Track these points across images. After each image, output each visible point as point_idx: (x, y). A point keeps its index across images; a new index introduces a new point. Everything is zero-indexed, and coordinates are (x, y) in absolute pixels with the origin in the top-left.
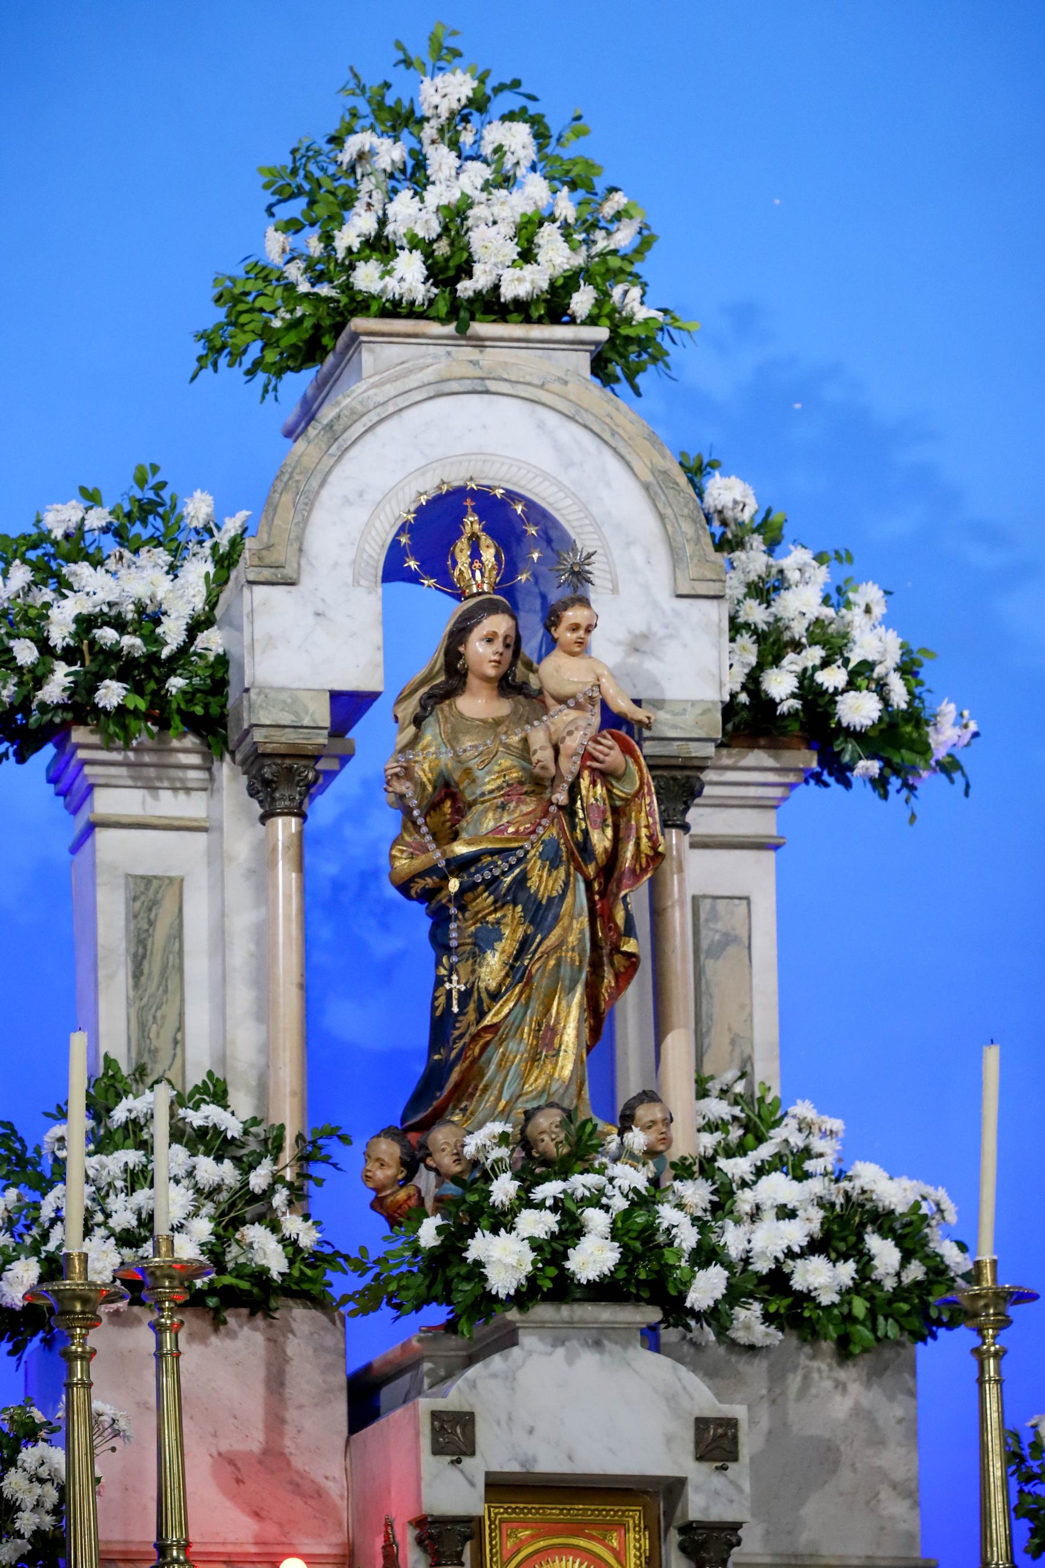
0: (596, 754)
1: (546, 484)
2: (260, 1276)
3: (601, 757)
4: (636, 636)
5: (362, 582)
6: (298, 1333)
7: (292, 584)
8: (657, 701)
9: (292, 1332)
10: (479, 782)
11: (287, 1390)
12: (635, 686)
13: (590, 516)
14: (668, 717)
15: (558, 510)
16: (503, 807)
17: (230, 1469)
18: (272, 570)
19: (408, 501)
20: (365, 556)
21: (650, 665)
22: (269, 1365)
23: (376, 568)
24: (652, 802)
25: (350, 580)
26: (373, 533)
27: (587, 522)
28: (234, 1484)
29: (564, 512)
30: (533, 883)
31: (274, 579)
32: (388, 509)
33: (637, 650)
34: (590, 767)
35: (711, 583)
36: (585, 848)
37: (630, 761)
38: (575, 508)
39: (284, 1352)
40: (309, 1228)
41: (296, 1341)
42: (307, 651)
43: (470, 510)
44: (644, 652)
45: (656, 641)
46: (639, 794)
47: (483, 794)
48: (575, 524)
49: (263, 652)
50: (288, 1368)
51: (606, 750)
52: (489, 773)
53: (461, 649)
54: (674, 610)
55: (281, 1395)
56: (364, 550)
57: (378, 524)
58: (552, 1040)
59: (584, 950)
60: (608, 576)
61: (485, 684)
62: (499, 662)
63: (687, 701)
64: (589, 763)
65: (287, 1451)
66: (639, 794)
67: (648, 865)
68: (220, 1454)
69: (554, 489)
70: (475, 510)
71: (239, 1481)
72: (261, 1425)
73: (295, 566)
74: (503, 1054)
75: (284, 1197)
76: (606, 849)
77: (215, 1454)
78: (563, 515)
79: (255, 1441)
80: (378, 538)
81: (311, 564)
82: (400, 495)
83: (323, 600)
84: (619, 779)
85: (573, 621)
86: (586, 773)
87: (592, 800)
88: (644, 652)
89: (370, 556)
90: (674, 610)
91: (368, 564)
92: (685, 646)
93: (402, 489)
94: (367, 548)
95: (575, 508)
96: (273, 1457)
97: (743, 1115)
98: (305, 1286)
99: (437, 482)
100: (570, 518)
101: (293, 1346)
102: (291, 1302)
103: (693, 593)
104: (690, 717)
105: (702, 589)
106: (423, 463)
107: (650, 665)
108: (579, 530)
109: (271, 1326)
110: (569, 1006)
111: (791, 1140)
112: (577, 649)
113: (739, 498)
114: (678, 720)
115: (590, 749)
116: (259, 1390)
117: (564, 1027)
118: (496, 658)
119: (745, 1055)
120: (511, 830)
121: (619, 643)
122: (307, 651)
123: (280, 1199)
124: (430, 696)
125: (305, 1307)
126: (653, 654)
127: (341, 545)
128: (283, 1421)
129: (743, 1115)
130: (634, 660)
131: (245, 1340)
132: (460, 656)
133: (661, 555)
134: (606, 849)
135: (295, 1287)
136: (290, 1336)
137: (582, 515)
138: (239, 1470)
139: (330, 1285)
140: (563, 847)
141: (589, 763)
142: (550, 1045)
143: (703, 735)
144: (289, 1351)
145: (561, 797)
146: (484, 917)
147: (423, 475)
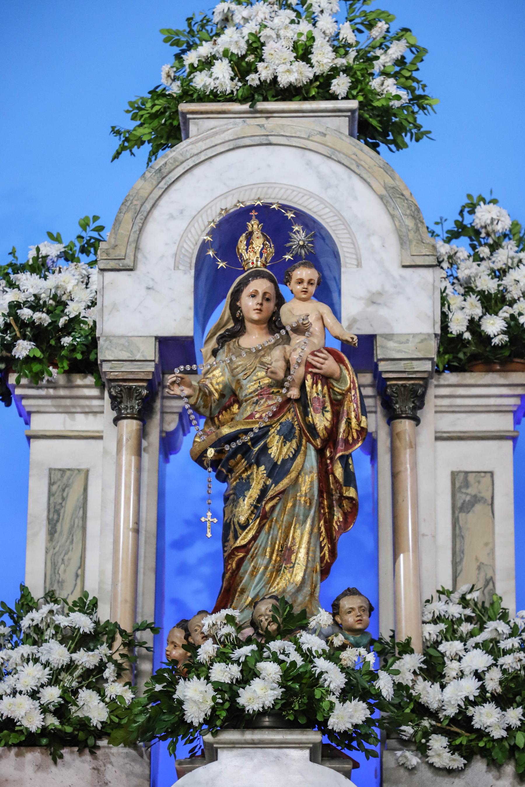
0: (314, 363)
1: (312, 200)
3: (318, 365)
5: (181, 267)
7: (131, 270)
8: (388, 335)
10: (244, 388)
12: (371, 325)
13: (342, 218)
14: (396, 345)
15: (320, 216)
16: (257, 402)
18: (116, 261)
19: (214, 215)
20: (183, 251)
23: (191, 258)
24: (356, 393)
25: (172, 267)
26: (190, 236)
27: (340, 222)
29: (324, 217)
30: (273, 451)
31: (117, 267)
32: (200, 220)
34: (311, 372)
35: (426, 257)
36: (312, 428)
37: (343, 368)
38: (331, 214)
42: (140, 312)
43: (254, 217)
45: (393, 299)
46: (349, 390)
47: (246, 395)
48: (331, 224)
49: (110, 314)
51: (321, 360)
52: (250, 381)
53: (238, 304)
54: (401, 276)
56: (183, 247)
57: (193, 230)
58: (290, 557)
59: (313, 495)
60: (354, 256)
61: (255, 326)
62: (260, 310)
63: (409, 334)
64: (310, 370)
66: (349, 390)
67: (358, 437)
69: (317, 203)
70: (257, 217)
73: (132, 258)
74: (254, 567)
76: (326, 428)
78: (324, 219)
80: (192, 240)
81: (145, 257)
82: (209, 211)
83: (153, 280)
84: (337, 380)
85: (299, 277)
86: (309, 377)
87: (315, 395)
88: (379, 304)
89: (187, 251)
90: (401, 276)
91: (185, 255)
92: (409, 299)
93: (211, 207)
94: (185, 246)
95: (331, 214)
97: (473, 615)
99: (235, 202)
100: (328, 221)
103: (413, 264)
104: (411, 345)
105: (419, 261)
106: (226, 191)
108: (334, 228)
110: (302, 534)
111: (499, 629)
112: (304, 296)
113: (495, 217)
114: (402, 347)
115: (310, 360)
117: (299, 548)
118: (258, 307)
119: (488, 577)
120: (257, 416)
122: (140, 312)
124: (222, 337)
127: (167, 244)
129: (473, 615)
132: (239, 308)
133: (393, 241)
134: (326, 428)
137: (336, 218)
140: (297, 428)
141: (310, 370)
142: (289, 560)
143: (420, 356)
145: (294, 393)
146: (240, 475)
147: (225, 198)
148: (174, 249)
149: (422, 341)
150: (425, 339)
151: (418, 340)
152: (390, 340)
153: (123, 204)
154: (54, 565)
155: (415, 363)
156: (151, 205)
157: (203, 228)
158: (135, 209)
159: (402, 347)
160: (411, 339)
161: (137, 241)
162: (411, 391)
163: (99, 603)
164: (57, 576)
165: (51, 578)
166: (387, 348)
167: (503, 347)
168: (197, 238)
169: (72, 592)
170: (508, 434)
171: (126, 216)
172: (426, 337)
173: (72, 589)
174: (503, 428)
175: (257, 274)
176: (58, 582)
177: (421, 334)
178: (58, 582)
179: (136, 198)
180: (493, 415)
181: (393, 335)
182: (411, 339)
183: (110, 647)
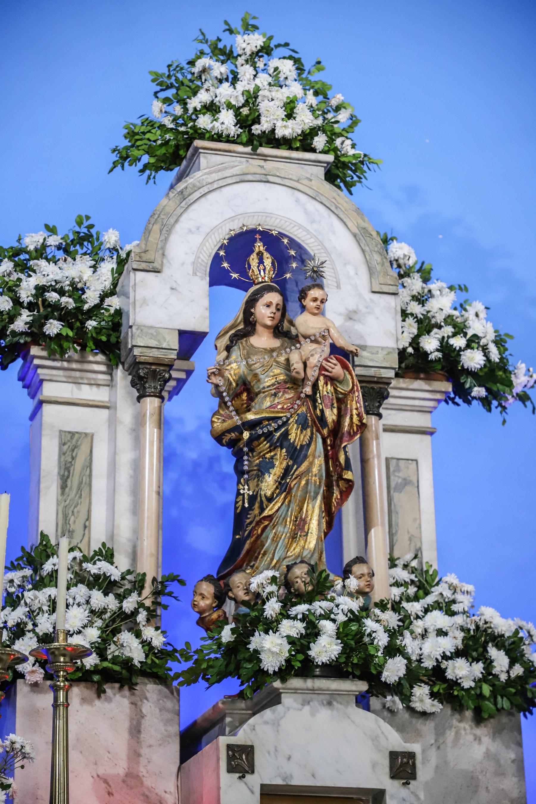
2: (127, 663)
4: (350, 311)
6: (150, 699)
9: (146, 699)
11: (142, 736)
21: (358, 327)
22: (131, 719)
26: (205, 249)
33: (351, 319)
39: (141, 711)
40: (158, 635)
41: (149, 704)
44: (355, 320)
50: (143, 721)
55: (138, 738)
57: (207, 244)
75: (144, 616)
88: (355, 320)
98: (155, 670)
101: (147, 708)
102: (146, 681)
107: (358, 327)
109: (133, 694)
116: (125, 735)
121: (340, 314)
123: (142, 617)
125: (155, 683)
126: (359, 321)
130: (349, 324)
131: (118, 702)
135: (149, 671)
136: (145, 701)
139: (170, 670)
144: (144, 711)
148: (192, 258)
149: (388, 354)
150: (391, 352)
151: (385, 352)
152: (364, 350)
153: (151, 216)
154: (66, 517)
155: (382, 370)
156: (175, 220)
157: (215, 243)
158: (162, 222)
159: (374, 357)
160: (380, 351)
161: (163, 248)
162: (378, 393)
164: (68, 526)
165: (63, 528)
166: (362, 357)
167: (438, 361)
168: (211, 251)
169: (81, 541)
170: (428, 430)
171: (154, 227)
172: (391, 350)
173: (81, 538)
174: (423, 425)
175: (268, 289)
176: (69, 531)
177: (387, 347)
178: (69, 531)
179: (163, 213)
180: (416, 414)
181: (366, 346)
182: (380, 351)
183: (140, 594)
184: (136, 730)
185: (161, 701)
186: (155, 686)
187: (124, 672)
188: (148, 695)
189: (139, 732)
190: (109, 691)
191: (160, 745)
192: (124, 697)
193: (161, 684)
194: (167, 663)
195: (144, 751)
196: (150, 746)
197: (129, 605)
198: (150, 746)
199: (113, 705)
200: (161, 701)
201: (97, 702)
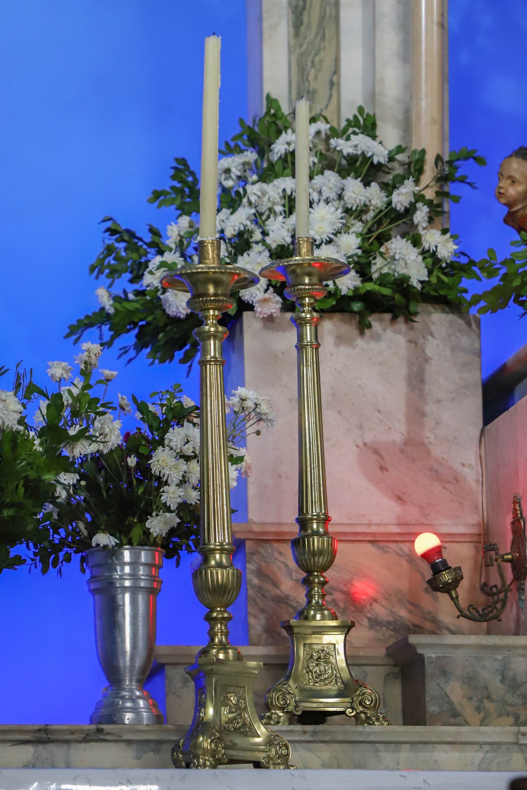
2: (401, 284)
11: (427, 387)
17: (374, 457)
22: (410, 364)
28: (379, 472)
39: (423, 351)
40: (447, 241)
50: (427, 367)
55: (421, 390)
65: (426, 441)
68: (365, 444)
71: (382, 468)
72: (403, 419)
75: (424, 214)
77: (361, 444)
79: (397, 433)
96: (413, 446)
98: (442, 293)
102: (430, 308)
109: (412, 328)
116: (402, 387)
123: (421, 215)
125: (444, 311)
128: (423, 414)
135: (433, 293)
138: (382, 458)
139: (466, 291)
154: (302, 71)
163: (378, 123)
164: (307, 84)
169: (326, 107)
176: (308, 92)
178: (308, 92)
183: (417, 182)
184: (417, 380)
185: (453, 338)
186: (443, 316)
187: (397, 296)
188: (433, 328)
189: (422, 381)
190: (376, 326)
191: (454, 399)
192: (399, 332)
193: (452, 312)
194: (460, 282)
195: (430, 408)
196: (439, 401)
197: (401, 198)
198: (439, 401)
199: (383, 345)
200: (453, 338)
201: (360, 342)
